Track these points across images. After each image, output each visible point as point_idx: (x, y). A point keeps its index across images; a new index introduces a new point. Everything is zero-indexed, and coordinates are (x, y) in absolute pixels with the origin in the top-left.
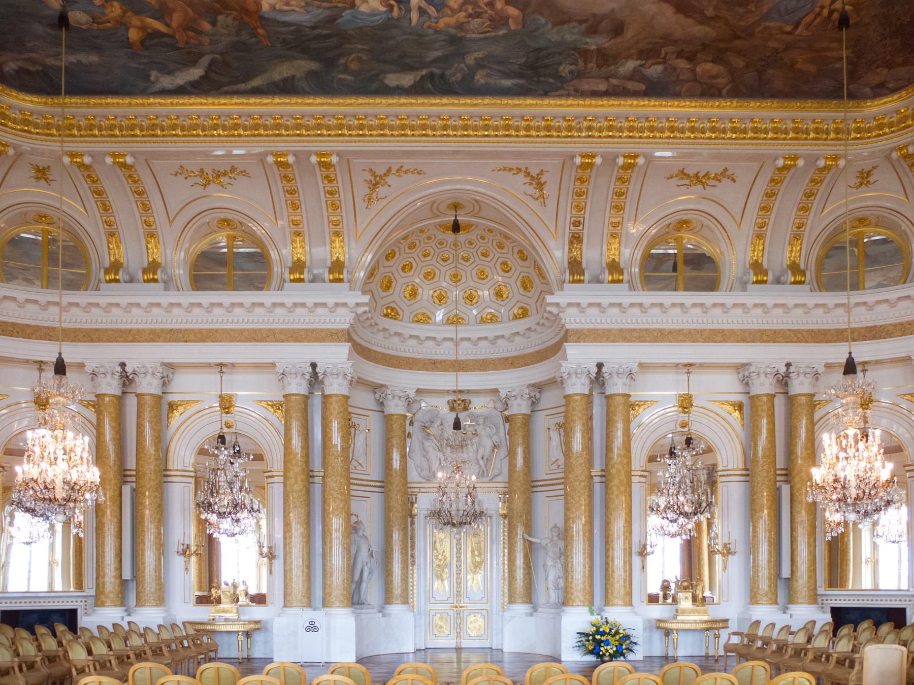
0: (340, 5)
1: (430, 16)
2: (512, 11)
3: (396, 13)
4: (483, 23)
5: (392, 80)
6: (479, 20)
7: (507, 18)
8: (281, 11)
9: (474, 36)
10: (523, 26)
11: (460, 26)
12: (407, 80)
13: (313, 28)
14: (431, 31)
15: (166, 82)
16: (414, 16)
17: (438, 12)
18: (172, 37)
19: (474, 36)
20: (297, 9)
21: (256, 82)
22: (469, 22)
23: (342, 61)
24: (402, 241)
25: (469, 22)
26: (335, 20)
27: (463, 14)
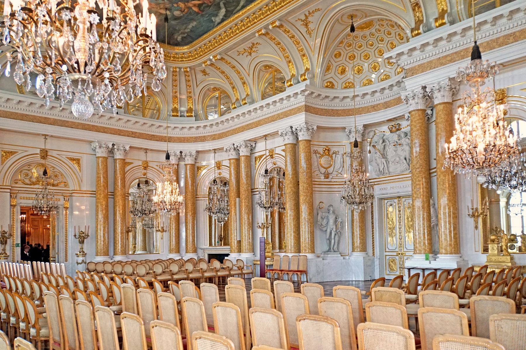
18: (202, 4)
24: (341, 45)
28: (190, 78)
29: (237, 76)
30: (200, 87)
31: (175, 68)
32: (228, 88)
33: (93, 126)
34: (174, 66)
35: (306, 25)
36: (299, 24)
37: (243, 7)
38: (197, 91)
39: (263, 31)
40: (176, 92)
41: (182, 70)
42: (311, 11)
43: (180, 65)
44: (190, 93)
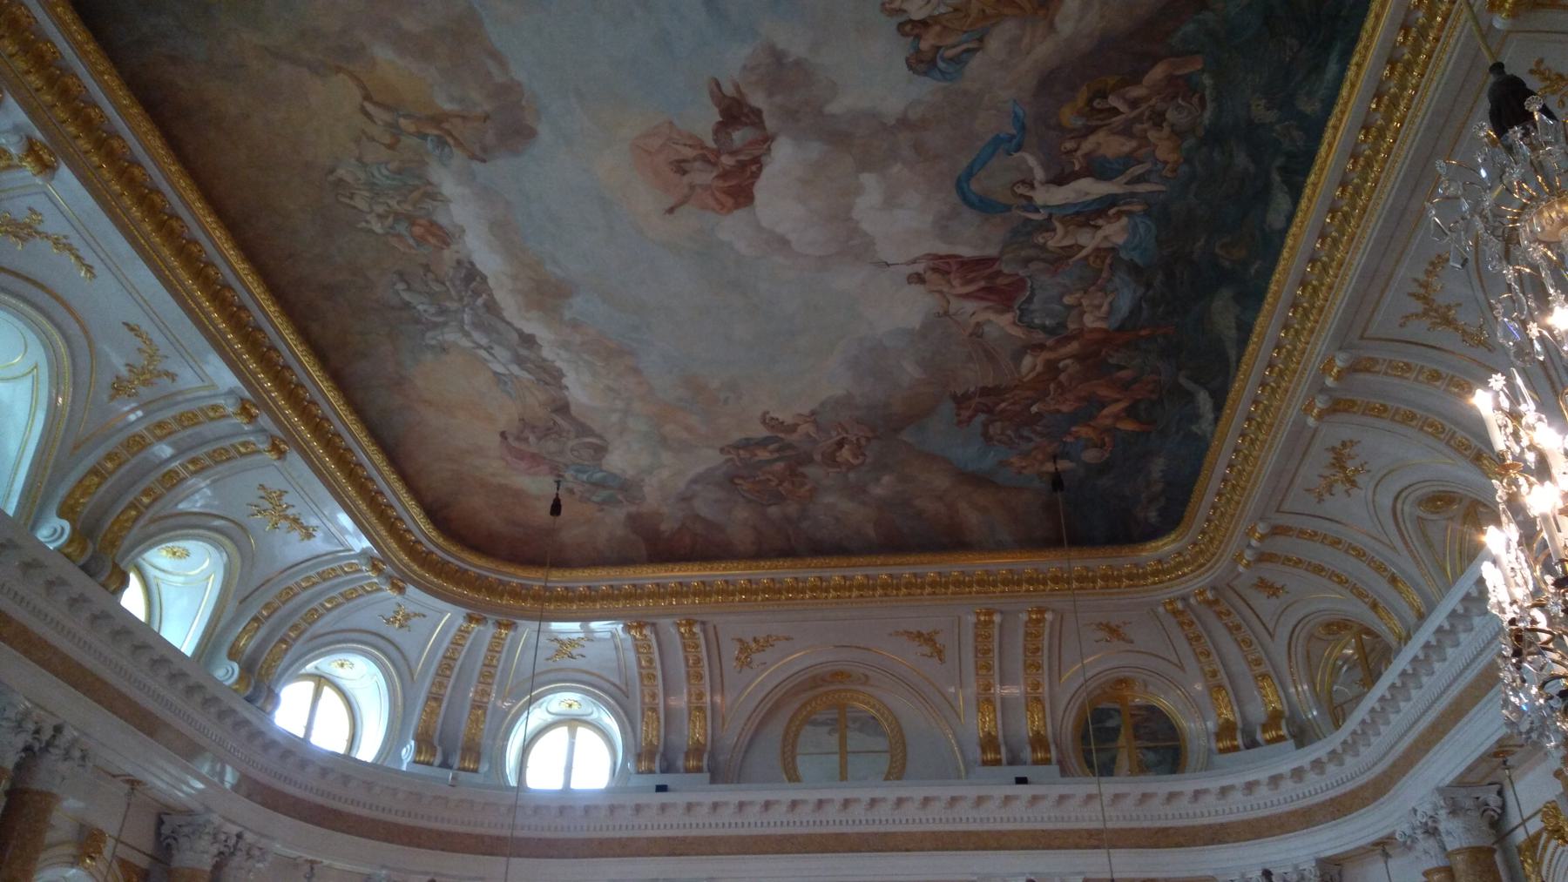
0: (1108, 261)
1: (1149, 172)
2: (1158, 72)
3: (1137, 208)
4: (1179, 106)
5: (1275, 219)
6: (1168, 116)
7: (1171, 80)
8: (1111, 312)
9: (1207, 114)
10: (1197, 52)
11: (1178, 134)
12: (1281, 201)
13: (1149, 286)
14: (1185, 168)
15: (1205, 426)
16: (1142, 188)
17: (1140, 162)
19: (1207, 114)
20: (1110, 299)
21: (1232, 354)
22: (1172, 126)
23: (1227, 264)
25: (1172, 126)
26: (1136, 266)
27: (1152, 135)
28: (1238, 619)
29: (1364, 566)
30: (1283, 633)
31: (1171, 602)
32: (1359, 611)
33: (967, 834)
34: (1166, 598)
35: (1448, 322)
36: (1419, 329)
37: (1239, 361)
38: (1278, 648)
39: (1320, 403)
40: (1214, 674)
41: (1192, 601)
42: (1422, 277)
43: (1179, 589)
44: (1258, 662)
